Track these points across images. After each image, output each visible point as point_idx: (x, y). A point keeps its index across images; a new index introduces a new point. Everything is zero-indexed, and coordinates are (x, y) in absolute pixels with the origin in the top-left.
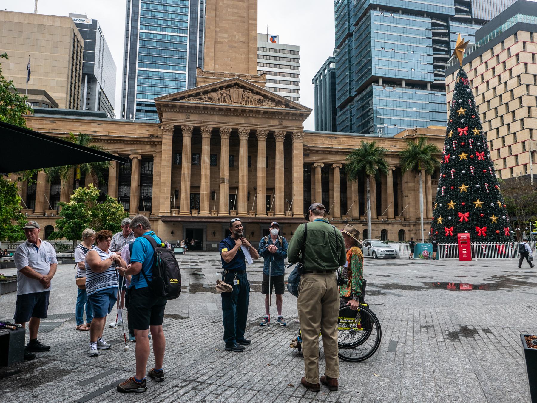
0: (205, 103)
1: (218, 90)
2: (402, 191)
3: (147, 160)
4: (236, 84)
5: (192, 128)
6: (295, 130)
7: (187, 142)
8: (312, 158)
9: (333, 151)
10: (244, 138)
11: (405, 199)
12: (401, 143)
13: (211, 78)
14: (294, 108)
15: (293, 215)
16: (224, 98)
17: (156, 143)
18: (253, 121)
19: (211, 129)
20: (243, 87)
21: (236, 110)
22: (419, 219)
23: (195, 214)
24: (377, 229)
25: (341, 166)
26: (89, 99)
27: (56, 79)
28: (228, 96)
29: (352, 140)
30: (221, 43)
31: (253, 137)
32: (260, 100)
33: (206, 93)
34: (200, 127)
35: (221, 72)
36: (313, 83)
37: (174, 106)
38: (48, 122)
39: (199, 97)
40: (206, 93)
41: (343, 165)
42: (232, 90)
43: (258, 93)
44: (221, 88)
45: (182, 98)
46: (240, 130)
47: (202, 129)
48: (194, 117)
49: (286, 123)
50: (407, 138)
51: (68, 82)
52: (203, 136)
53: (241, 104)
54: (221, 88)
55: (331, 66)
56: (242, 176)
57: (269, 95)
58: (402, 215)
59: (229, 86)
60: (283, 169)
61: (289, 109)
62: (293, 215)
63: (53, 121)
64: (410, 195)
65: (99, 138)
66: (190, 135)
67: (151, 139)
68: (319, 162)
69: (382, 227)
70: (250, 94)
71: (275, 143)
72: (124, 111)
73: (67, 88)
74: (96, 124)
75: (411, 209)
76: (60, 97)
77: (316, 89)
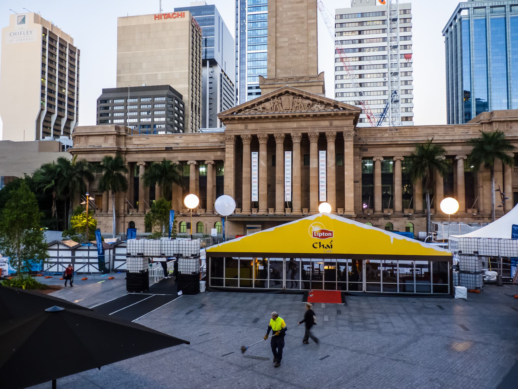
3: (219, 164)
4: (287, 92)
5: (250, 136)
6: (345, 129)
8: (371, 152)
10: (297, 141)
11: (481, 189)
12: (475, 128)
13: (273, 84)
15: (344, 212)
17: (223, 150)
18: (304, 124)
19: (266, 136)
21: (287, 117)
22: (492, 211)
23: (254, 213)
27: (180, 71)
29: (416, 130)
30: (282, 47)
31: (305, 140)
32: (309, 104)
33: (261, 103)
34: (256, 135)
35: (281, 76)
36: (444, 35)
37: (233, 119)
38: (144, 139)
40: (261, 103)
42: (283, 98)
44: (273, 97)
45: (240, 111)
47: (258, 136)
48: (252, 126)
49: (336, 123)
50: (482, 123)
51: (189, 73)
52: (260, 142)
54: (273, 97)
55: (464, 13)
56: (295, 177)
58: (477, 207)
59: (281, 95)
60: (334, 168)
62: (344, 212)
64: (485, 187)
67: (220, 146)
73: (189, 78)
74: (178, 137)
75: (486, 201)
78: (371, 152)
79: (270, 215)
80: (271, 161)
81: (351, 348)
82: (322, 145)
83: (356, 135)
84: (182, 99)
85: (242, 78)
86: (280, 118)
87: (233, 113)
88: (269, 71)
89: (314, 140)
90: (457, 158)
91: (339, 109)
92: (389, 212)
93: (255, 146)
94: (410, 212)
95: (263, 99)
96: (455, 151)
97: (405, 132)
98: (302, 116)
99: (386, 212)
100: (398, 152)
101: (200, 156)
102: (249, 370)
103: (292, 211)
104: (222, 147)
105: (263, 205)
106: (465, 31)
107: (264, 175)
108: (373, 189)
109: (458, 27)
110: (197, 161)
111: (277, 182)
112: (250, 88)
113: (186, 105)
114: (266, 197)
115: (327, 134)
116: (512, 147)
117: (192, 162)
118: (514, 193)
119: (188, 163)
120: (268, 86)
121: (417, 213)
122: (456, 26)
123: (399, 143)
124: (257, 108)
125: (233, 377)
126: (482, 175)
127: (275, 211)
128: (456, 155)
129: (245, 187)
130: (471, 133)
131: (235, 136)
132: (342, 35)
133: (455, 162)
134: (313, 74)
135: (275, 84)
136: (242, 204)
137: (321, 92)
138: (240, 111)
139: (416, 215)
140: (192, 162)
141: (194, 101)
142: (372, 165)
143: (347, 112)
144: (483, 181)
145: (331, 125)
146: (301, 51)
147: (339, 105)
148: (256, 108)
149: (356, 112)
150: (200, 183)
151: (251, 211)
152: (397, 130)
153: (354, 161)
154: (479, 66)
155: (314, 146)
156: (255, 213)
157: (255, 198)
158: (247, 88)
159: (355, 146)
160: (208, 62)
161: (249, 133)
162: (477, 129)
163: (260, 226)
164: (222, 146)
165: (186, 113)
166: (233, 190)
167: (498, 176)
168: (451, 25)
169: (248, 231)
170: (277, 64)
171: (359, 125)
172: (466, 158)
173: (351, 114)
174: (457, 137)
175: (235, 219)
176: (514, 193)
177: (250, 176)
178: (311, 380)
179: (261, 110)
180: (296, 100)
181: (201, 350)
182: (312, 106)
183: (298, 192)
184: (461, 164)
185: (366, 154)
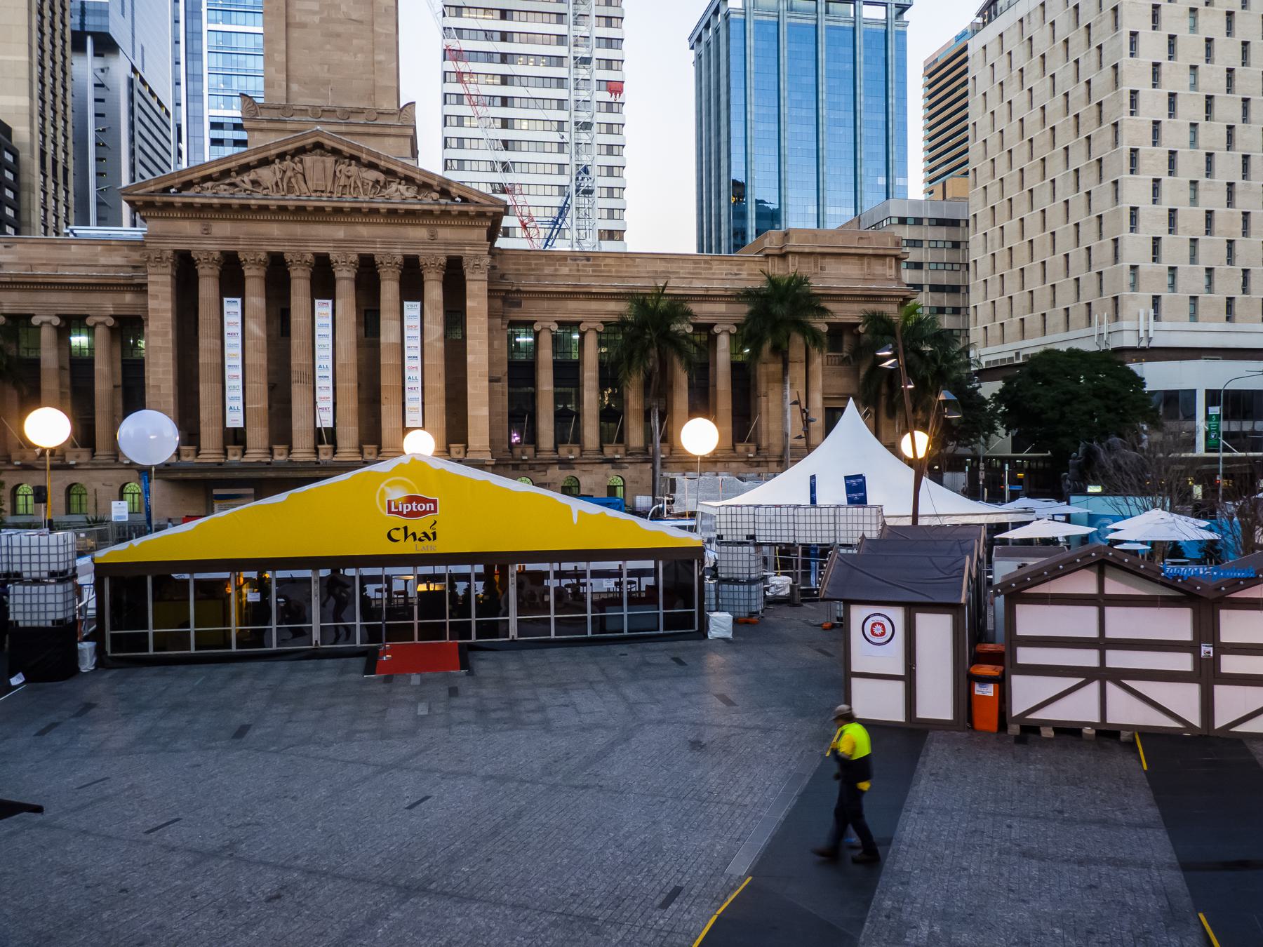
0: (243, 195)
1: (273, 162)
3: (128, 327)
4: (318, 146)
5: (217, 255)
6: (468, 251)
8: (530, 310)
9: (579, 293)
10: (345, 274)
12: (753, 266)
13: (279, 121)
17: (141, 289)
18: (363, 231)
19: (263, 256)
22: (785, 448)
23: (234, 457)
26: (102, 100)
28: (299, 176)
29: (630, 262)
30: (303, 26)
31: (368, 272)
32: (378, 182)
33: (246, 168)
35: (302, 101)
36: (692, 48)
37: (170, 206)
39: (227, 181)
40: (246, 168)
42: (308, 159)
43: (372, 166)
44: (282, 156)
45: (188, 185)
46: (333, 257)
48: (223, 228)
49: (445, 234)
50: (767, 256)
51: (31, 64)
52: (247, 273)
56: (343, 365)
57: (399, 169)
58: (755, 440)
59: (302, 151)
60: (440, 345)
64: (771, 396)
65: (8, 279)
66: (217, 273)
67: (132, 277)
70: (354, 169)
71: (423, 283)
72: (179, 140)
75: (774, 427)
78: (530, 310)
79: (279, 463)
80: (277, 323)
81: (482, 772)
82: (412, 288)
83: (493, 267)
84: (9, 137)
85: (195, 97)
86: (301, 213)
87: (166, 190)
88: (268, 84)
89: (390, 275)
90: (716, 330)
91: (453, 199)
92: (571, 452)
93: (232, 282)
94: (616, 452)
95: (252, 159)
96: (712, 314)
98: (358, 210)
99: (563, 451)
100: (589, 312)
101: (70, 302)
102: (222, 859)
103: (335, 453)
104: (136, 281)
105: (258, 437)
106: (736, 44)
107: (259, 359)
108: (533, 397)
109: (723, 33)
110: (62, 317)
111: (294, 377)
112: (214, 126)
113: (24, 156)
114: (264, 416)
115: (422, 260)
116: (823, 311)
117: (46, 318)
118: (827, 409)
119: (35, 321)
120: (265, 125)
121: (631, 454)
122: (717, 31)
124: (237, 180)
125: (178, 882)
126: (767, 369)
127: (290, 453)
128: (714, 324)
129: (206, 391)
130: (744, 275)
131: (175, 251)
132: (459, 15)
133: (713, 339)
134: (387, 105)
135: (285, 121)
136: (198, 434)
137: (409, 153)
138: (188, 185)
139: (629, 459)
140: (45, 320)
141: (49, 148)
142: (530, 340)
143: (471, 209)
144: (768, 382)
145: (433, 236)
146: (355, 42)
147: (453, 191)
148: (233, 180)
150: (73, 378)
151: (226, 453)
152: (588, 260)
153: (490, 330)
154: (763, 128)
155: (389, 289)
156: (236, 458)
157: (235, 419)
158: (207, 126)
159: (492, 293)
160: (89, 39)
161: (214, 247)
162: (756, 268)
163: (251, 491)
164: (137, 277)
165: (24, 179)
166: (172, 399)
167: (797, 371)
168: (707, 26)
169: (216, 506)
170: (291, 67)
171: (501, 243)
172: (734, 330)
173: (481, 215)
174: (716, 284)
175: (180, 475)
176: (827, 409)
177: (219, 361)
178: (384, 860)
179: (249, 186)
180: (343, 167)
181: (83, 826)
182: (385, 187)
183: (350, 404)
184: (723, 342)
185: (516, 314)
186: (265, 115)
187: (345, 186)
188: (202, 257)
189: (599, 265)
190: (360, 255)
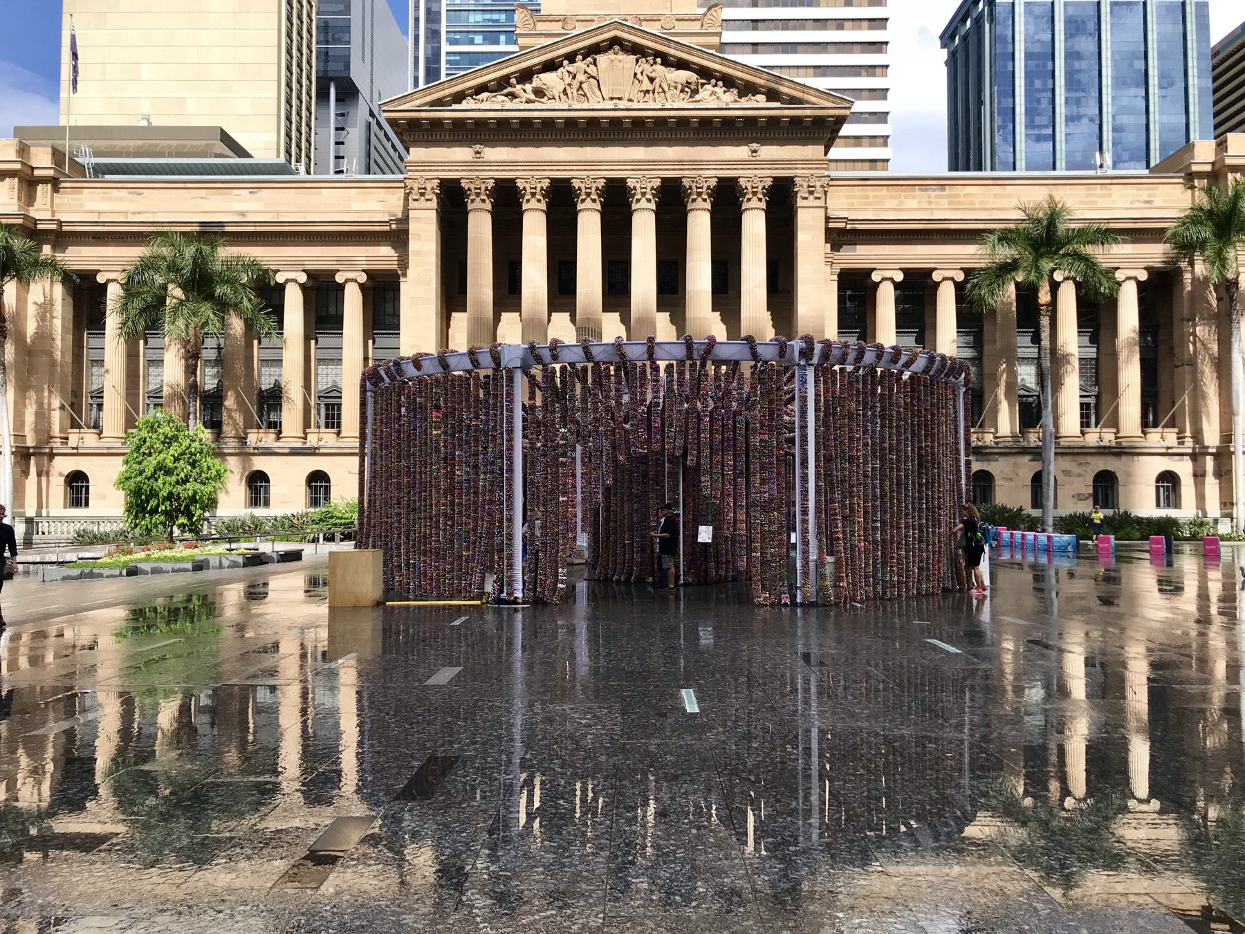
2: (1172, 348)
4: (615, 42)
6: (798, 172)
7: (480, 228)
14: (793, 100)
16: (580, 87)
20: (637, 50)
21: (615, 123)
24: (1079, 470)
25: (960, 277)
33: (526, 76)
36: (943, 46)
37: (436, 124)
40: (526, 76)
41: (968, 272)
42: (601, 58)
43: (681, 65)
44: (571, 58)
45: (459, 97)
53: (630, 100)
54: (571, 58)
59: (594, 50)
61: (778, 105)
63: (137, 188)
65: (252, 229)
68: (887, 264)
69: (1100, 464)
70: (659, 68)
76: (262, 141)
77: (952, 63)
97: (966, 195)
101: (320, 256)
117: (291, 275)
123: (953, 227)
149: (837, 112)
173: (819, 122)
179: (532, 97)
182: (696, 92)
186: (542, 27)
187: (648, 92)
188: (472, 186)
189: (959, 196)
190: (664, 180)
